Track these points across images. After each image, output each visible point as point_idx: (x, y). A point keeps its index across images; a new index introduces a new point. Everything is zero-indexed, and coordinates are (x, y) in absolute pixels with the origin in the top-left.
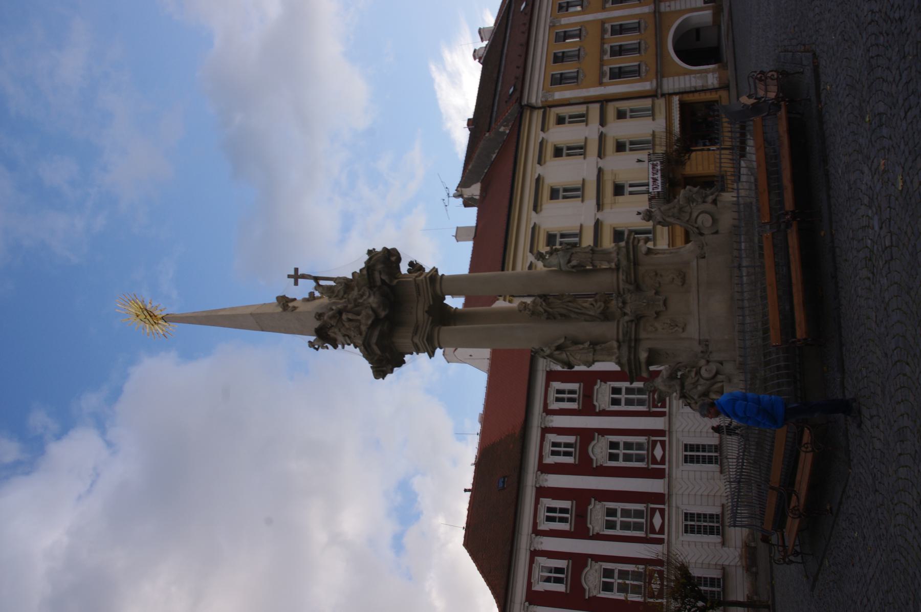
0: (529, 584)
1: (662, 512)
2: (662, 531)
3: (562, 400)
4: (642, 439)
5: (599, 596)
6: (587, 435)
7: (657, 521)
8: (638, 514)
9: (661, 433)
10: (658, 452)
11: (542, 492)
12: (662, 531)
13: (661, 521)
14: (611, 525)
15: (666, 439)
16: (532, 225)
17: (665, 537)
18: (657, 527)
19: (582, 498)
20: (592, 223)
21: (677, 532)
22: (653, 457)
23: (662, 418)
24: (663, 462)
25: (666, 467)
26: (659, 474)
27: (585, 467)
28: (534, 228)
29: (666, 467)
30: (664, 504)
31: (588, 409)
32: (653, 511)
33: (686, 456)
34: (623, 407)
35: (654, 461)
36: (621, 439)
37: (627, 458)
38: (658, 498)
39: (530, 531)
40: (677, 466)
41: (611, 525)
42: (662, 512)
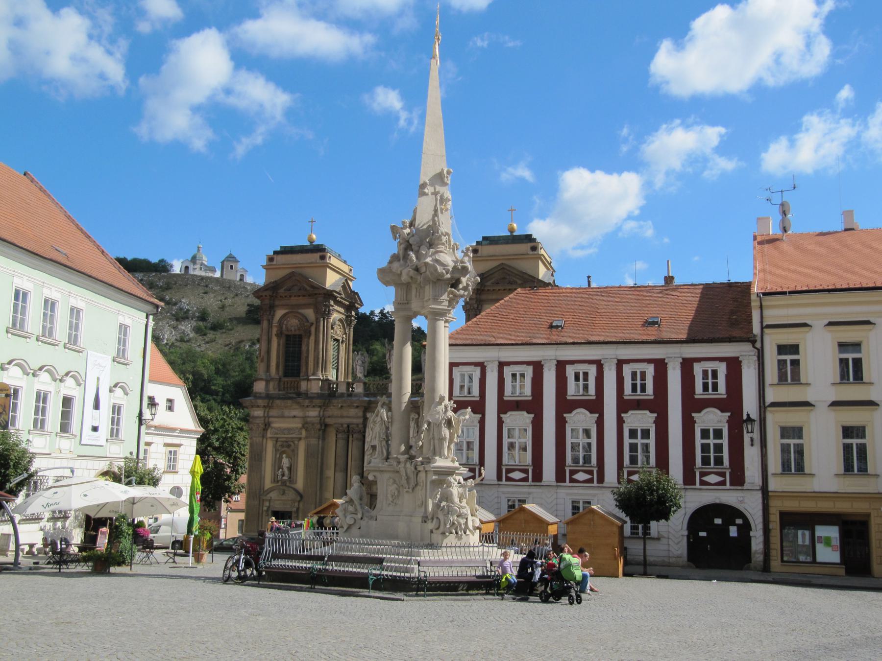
1: (525, 480)
2: (509, 479)
6: (596, 406)
9: (601, 479)
10: (581, 476)
11: (538, 367)
12: (509, 479)
15: (595, 484)
16: (872, 320)
17: (504, 482)
18: (511, 475)
19: (534, 406)
20: (809, 399)
21: (508, 493)
22: (576, 472)
23: (616, 481)
25: (567, 483)
26: (560, 476)
27: (565, 406)
28: (868, 323)
29: (567, 483)
30: (533, 481)
31: (624, 406)
33: (579, 502)
34: (627, 441)
35: (573, 472)
38: (538, 476)
39: (503, 360)
40: (567, 494)
41: (633, 433)
42: (525, 480)
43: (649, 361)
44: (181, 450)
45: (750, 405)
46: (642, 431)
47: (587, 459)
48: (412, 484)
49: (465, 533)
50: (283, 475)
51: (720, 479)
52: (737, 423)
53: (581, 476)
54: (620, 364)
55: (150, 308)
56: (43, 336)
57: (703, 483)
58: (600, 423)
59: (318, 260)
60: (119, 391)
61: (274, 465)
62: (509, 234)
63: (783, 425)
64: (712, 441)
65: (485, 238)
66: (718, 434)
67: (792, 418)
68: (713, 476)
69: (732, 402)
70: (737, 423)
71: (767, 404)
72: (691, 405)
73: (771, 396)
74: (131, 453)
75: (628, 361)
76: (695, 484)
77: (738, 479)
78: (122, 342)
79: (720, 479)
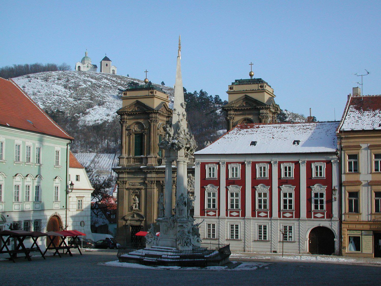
0: (208, 163)
1: (238, 216)
2: (231, 216)
3: (286, 170)
4: (268, 207)
5: (206, 191)
6: (268, 183)
7: (235, 214)
8: (237, 206)
9: (271, 216)
10: (262, 214)
12: (231, 216)
13: (235, 215)
14: (232, 195)
19: (242, 182)
21: (231, 222)
24: (259, 216)
25: (257, 217)
26: (253, 215)
27: (255, 182)
31: (281, 182)
32: (238, 212)
35: (259, 213)
36: (268, 198)
37: (260, 201)
38: (244, 214)
40: (257, 222)
42: (238, 216)
43: (292, 162)
44: (84, 199)
45: (335, 183)
46: (289, 194)
47: (265, 207)
48: (173, 226)
49: (190, 245)
50: (136, 207)
51: (322, 215)
52: (330, 191)
53: (262, 214)
54: (280, 163)
55: (68, 141)
56: (27, 162)
57: (315, 217)
58: (271, 190)
59: (150, 94)
60: (57, 180)
61: (129, 202)
62: (249, 78)
63: (349, 191)
64: (319, 199)
65: (236, 81)
66: (322, 195)
67: (353, 189)
68: (319, 214)
69: (328, 181)
70: (330, 191)
71: (342, 182)
72: (311, 182)
73: (344, 178)
74: (63, 207)
75: (283, 162)
76: (311, 218)
77: (330, 216)
78: (57, 158)
79: (322, 215)
